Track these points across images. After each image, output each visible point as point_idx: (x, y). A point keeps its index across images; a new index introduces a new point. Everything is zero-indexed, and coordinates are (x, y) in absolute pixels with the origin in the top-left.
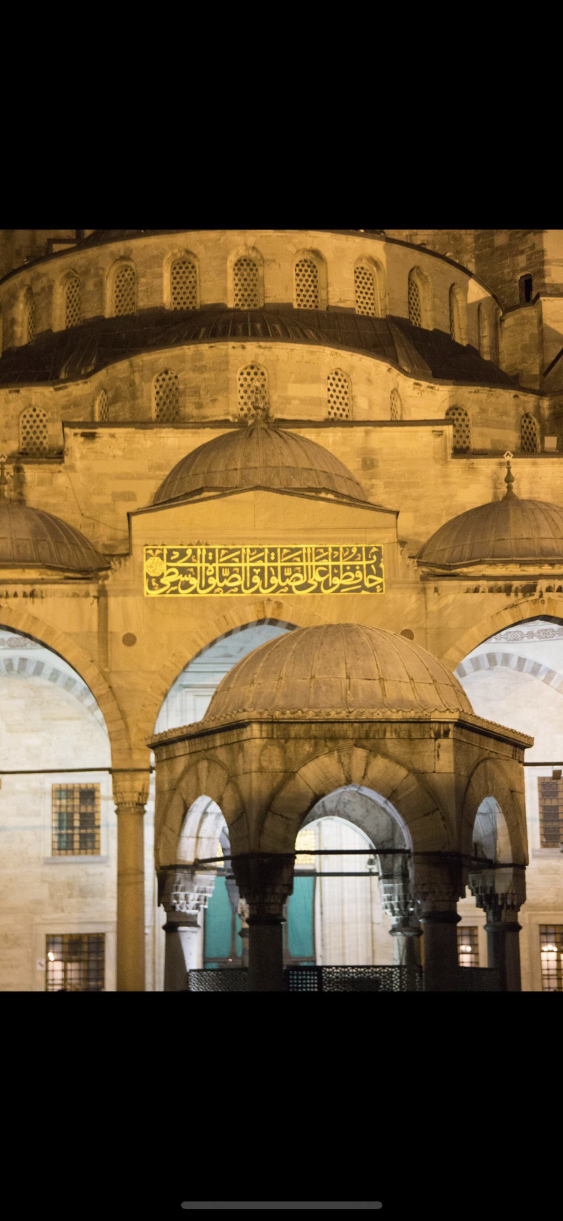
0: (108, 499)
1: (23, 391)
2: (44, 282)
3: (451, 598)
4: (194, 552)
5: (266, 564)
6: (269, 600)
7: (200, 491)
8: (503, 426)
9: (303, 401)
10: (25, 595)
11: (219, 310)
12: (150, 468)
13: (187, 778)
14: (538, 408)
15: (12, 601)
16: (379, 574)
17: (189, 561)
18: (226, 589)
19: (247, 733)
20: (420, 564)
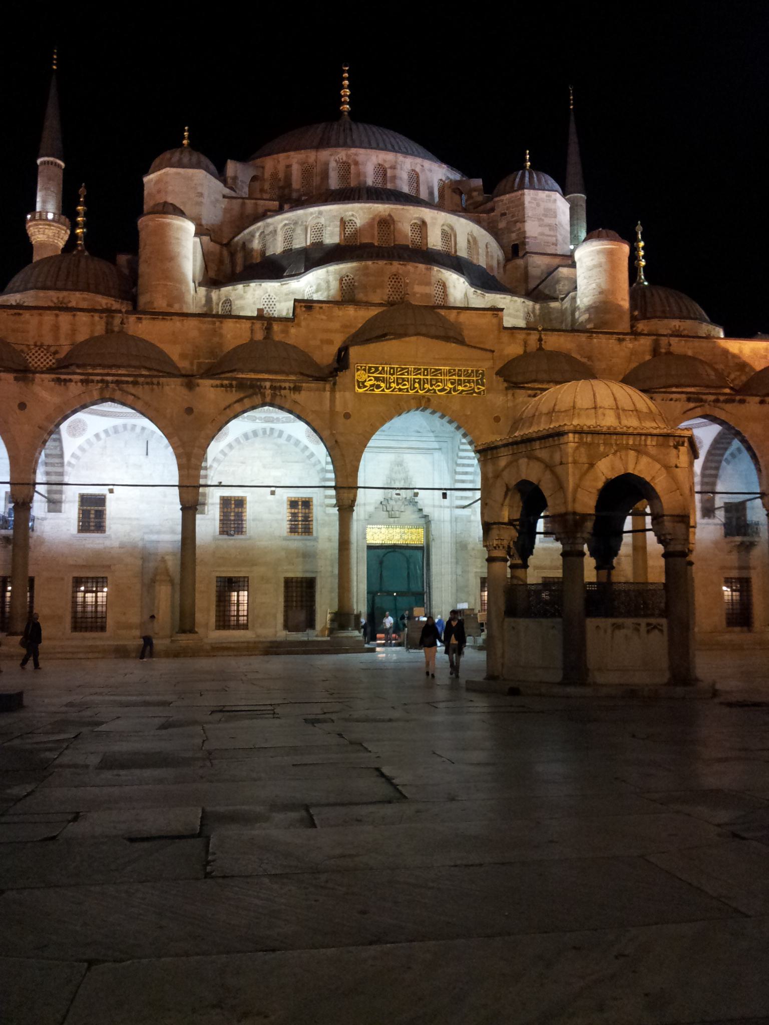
0: (318, 343)
1: (264, 285)
2: (271, 228)
3: (521, 399)
4: (383, 368)
5: (422, 377)
6: (423, 397)
7: (384, 335)
8: (516, 317)
9: (422, 295)
10: (290, 389)
11: (371, 245)
12: (342, 326)
13: (508, 470)
14: (534, 308)
15: (283, 392)
16: (483, 385)
17: (380, 373)
18: (400, 390)
19: (564, 439)
20: (505, 381)
